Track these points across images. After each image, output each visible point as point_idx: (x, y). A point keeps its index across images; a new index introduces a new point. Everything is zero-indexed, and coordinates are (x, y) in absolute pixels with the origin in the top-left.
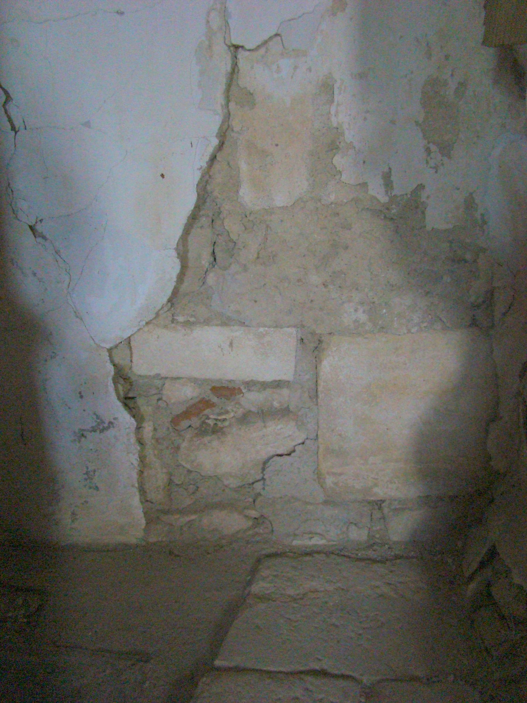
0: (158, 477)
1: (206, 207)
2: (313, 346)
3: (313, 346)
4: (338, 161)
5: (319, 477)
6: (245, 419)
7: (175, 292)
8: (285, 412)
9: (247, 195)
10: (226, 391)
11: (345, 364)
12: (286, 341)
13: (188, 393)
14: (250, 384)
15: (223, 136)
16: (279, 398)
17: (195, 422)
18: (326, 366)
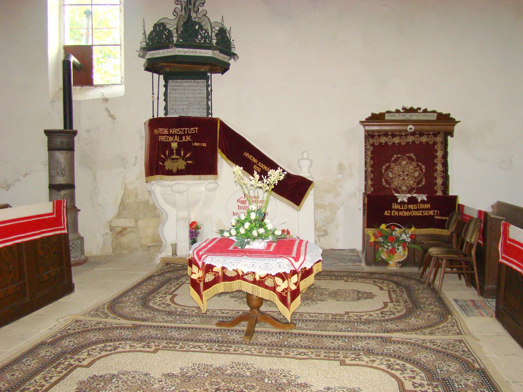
0: (115, 244)
1: (122, 203)
2: (137, 221)
3: (137, 221)
4: (138, 196)
5: (139, 242)
6: (128, 233)
7: (118, 214)
8: (133, 232)
9: (127, 200)
10: (125, 229)
11: (141, 223)
12: (133, 220)
13: (119, 229)
14: (128, 227)
15: (124, 194)
16: (133, 229)
17: (120, 234)
18: (138, 223)
